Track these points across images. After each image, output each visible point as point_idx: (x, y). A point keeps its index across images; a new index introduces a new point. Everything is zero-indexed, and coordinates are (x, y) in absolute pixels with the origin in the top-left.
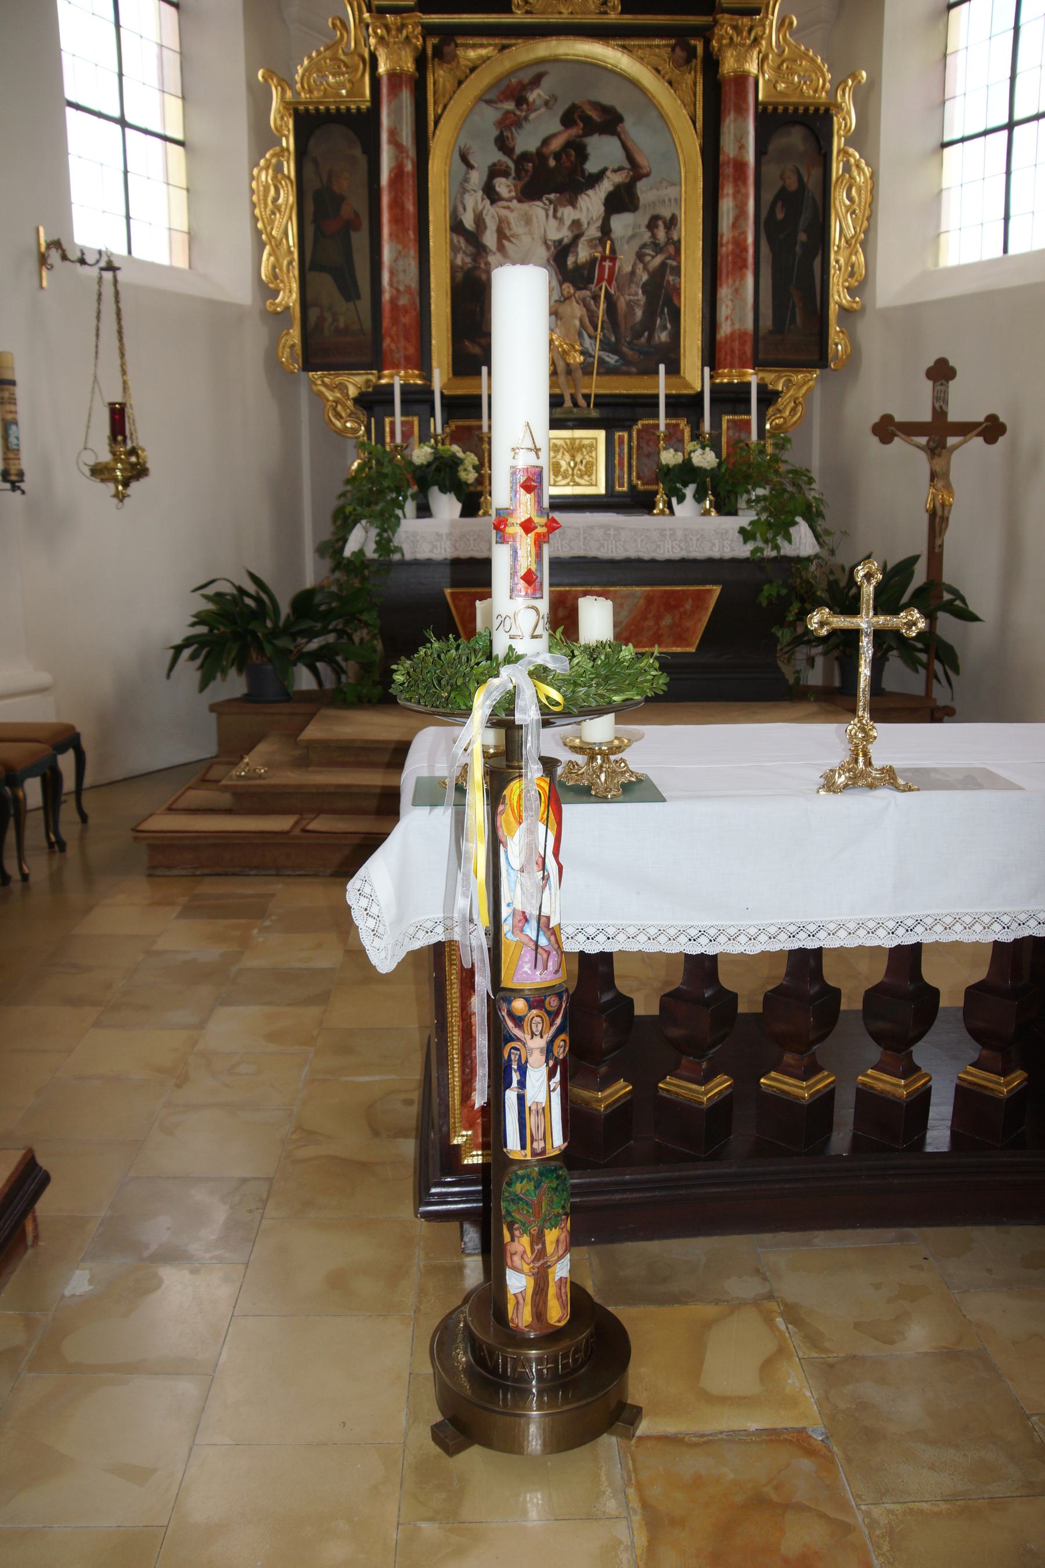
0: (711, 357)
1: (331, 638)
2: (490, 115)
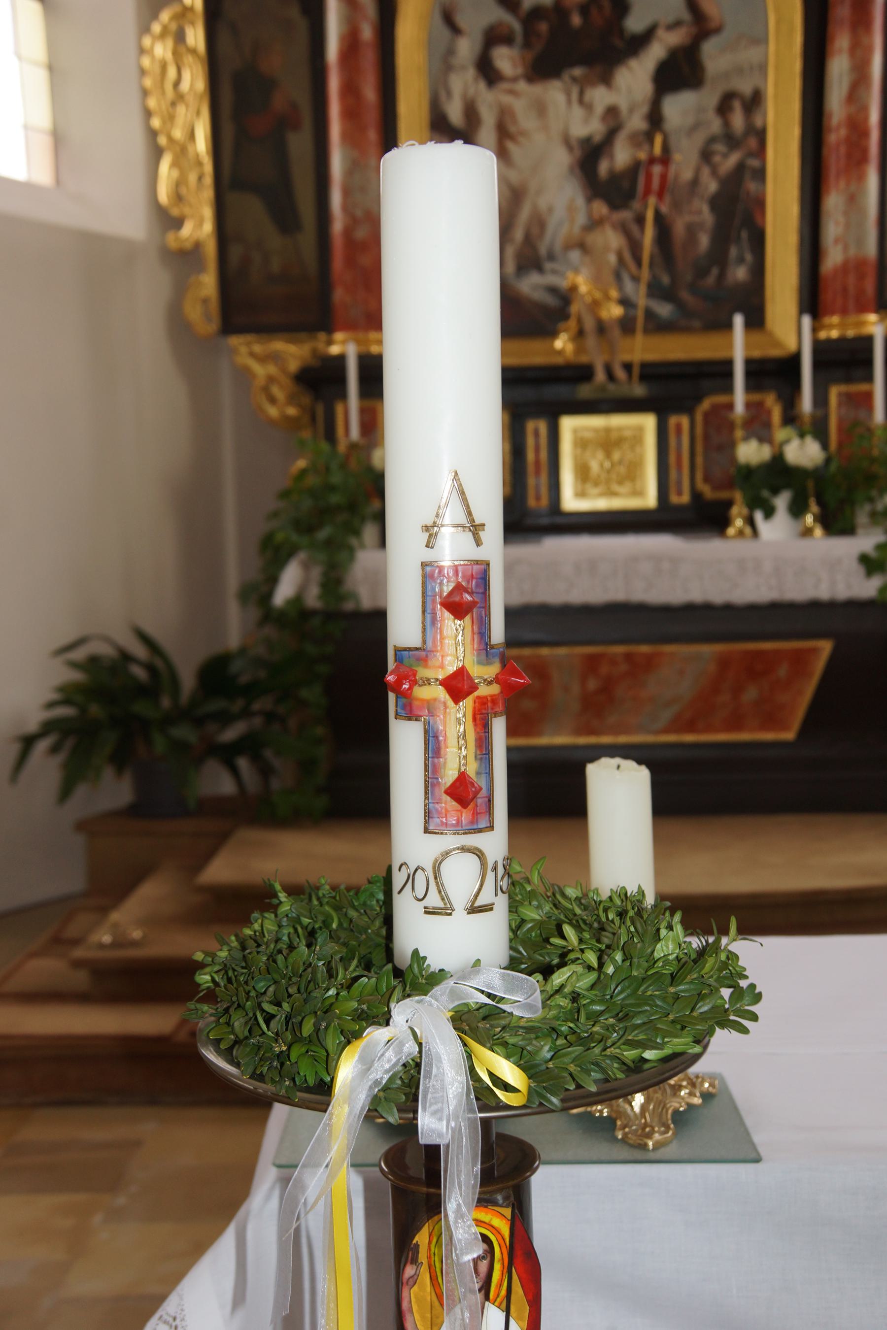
0: (813, 301)
1: (257, 721)
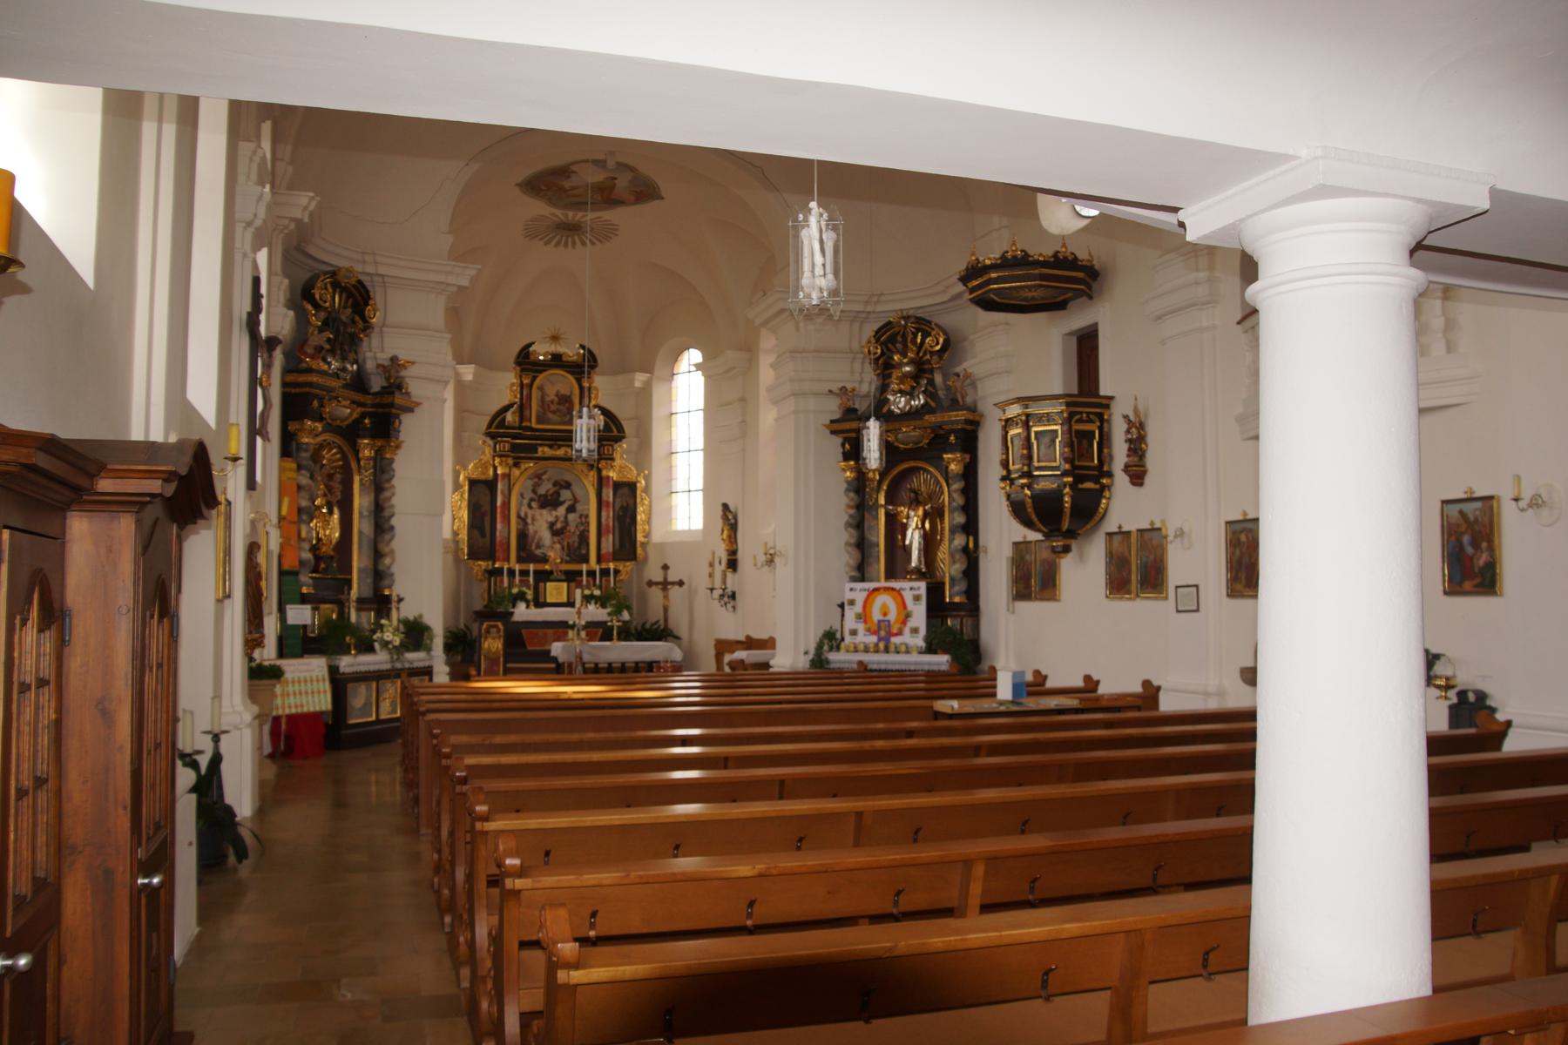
2: (530, 483)
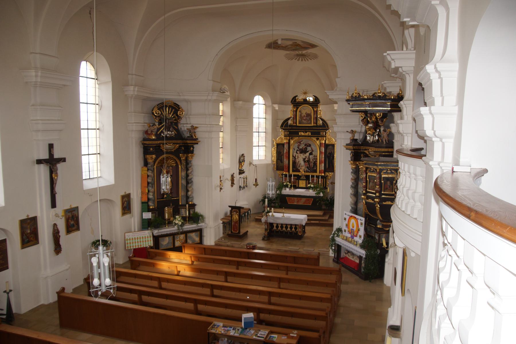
2: (296, 145)
